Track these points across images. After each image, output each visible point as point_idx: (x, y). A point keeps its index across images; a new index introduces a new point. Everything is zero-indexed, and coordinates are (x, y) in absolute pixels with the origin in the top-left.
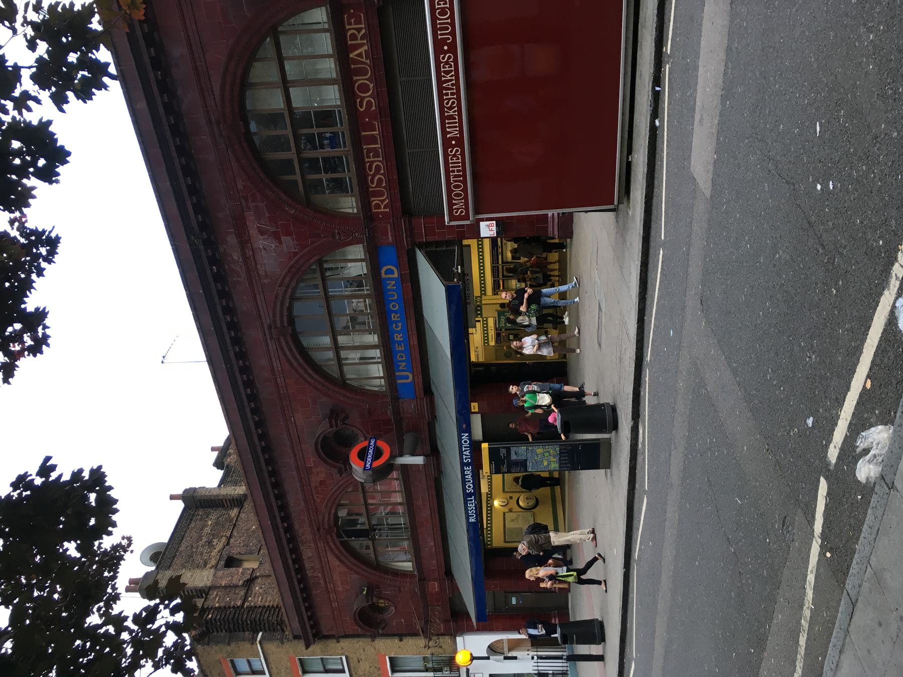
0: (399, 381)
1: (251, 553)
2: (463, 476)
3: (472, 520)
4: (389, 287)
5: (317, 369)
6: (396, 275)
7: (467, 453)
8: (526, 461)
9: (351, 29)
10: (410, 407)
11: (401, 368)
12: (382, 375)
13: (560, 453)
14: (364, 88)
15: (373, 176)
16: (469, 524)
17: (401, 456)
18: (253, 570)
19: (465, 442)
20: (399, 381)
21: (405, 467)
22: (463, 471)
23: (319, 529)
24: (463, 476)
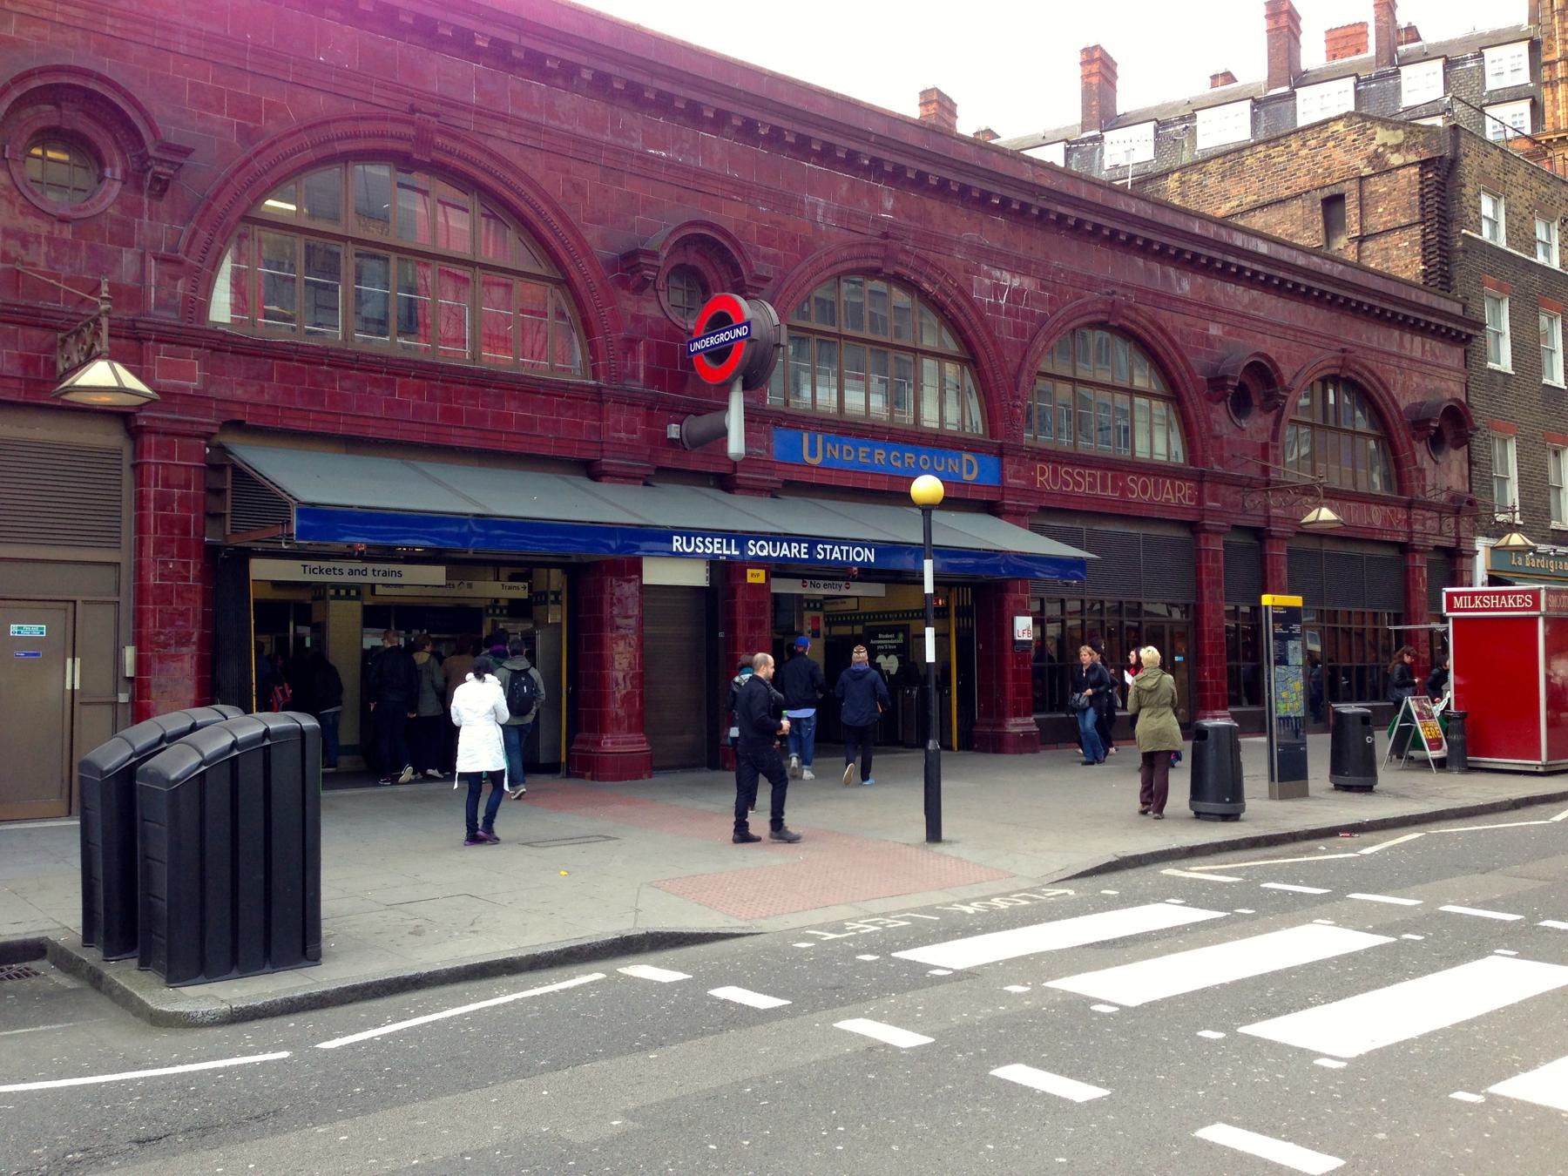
0: (806, 437)
2: (790, 538)
6: (966, 477)
8: (1286, 663)
9: (1187, 488)
11: (829, 447)
14: (1145, 491)
15: (1071, 475)
19: (858, 554)
20: (806, 437)
22: (799, 539)
24: (790, 538)
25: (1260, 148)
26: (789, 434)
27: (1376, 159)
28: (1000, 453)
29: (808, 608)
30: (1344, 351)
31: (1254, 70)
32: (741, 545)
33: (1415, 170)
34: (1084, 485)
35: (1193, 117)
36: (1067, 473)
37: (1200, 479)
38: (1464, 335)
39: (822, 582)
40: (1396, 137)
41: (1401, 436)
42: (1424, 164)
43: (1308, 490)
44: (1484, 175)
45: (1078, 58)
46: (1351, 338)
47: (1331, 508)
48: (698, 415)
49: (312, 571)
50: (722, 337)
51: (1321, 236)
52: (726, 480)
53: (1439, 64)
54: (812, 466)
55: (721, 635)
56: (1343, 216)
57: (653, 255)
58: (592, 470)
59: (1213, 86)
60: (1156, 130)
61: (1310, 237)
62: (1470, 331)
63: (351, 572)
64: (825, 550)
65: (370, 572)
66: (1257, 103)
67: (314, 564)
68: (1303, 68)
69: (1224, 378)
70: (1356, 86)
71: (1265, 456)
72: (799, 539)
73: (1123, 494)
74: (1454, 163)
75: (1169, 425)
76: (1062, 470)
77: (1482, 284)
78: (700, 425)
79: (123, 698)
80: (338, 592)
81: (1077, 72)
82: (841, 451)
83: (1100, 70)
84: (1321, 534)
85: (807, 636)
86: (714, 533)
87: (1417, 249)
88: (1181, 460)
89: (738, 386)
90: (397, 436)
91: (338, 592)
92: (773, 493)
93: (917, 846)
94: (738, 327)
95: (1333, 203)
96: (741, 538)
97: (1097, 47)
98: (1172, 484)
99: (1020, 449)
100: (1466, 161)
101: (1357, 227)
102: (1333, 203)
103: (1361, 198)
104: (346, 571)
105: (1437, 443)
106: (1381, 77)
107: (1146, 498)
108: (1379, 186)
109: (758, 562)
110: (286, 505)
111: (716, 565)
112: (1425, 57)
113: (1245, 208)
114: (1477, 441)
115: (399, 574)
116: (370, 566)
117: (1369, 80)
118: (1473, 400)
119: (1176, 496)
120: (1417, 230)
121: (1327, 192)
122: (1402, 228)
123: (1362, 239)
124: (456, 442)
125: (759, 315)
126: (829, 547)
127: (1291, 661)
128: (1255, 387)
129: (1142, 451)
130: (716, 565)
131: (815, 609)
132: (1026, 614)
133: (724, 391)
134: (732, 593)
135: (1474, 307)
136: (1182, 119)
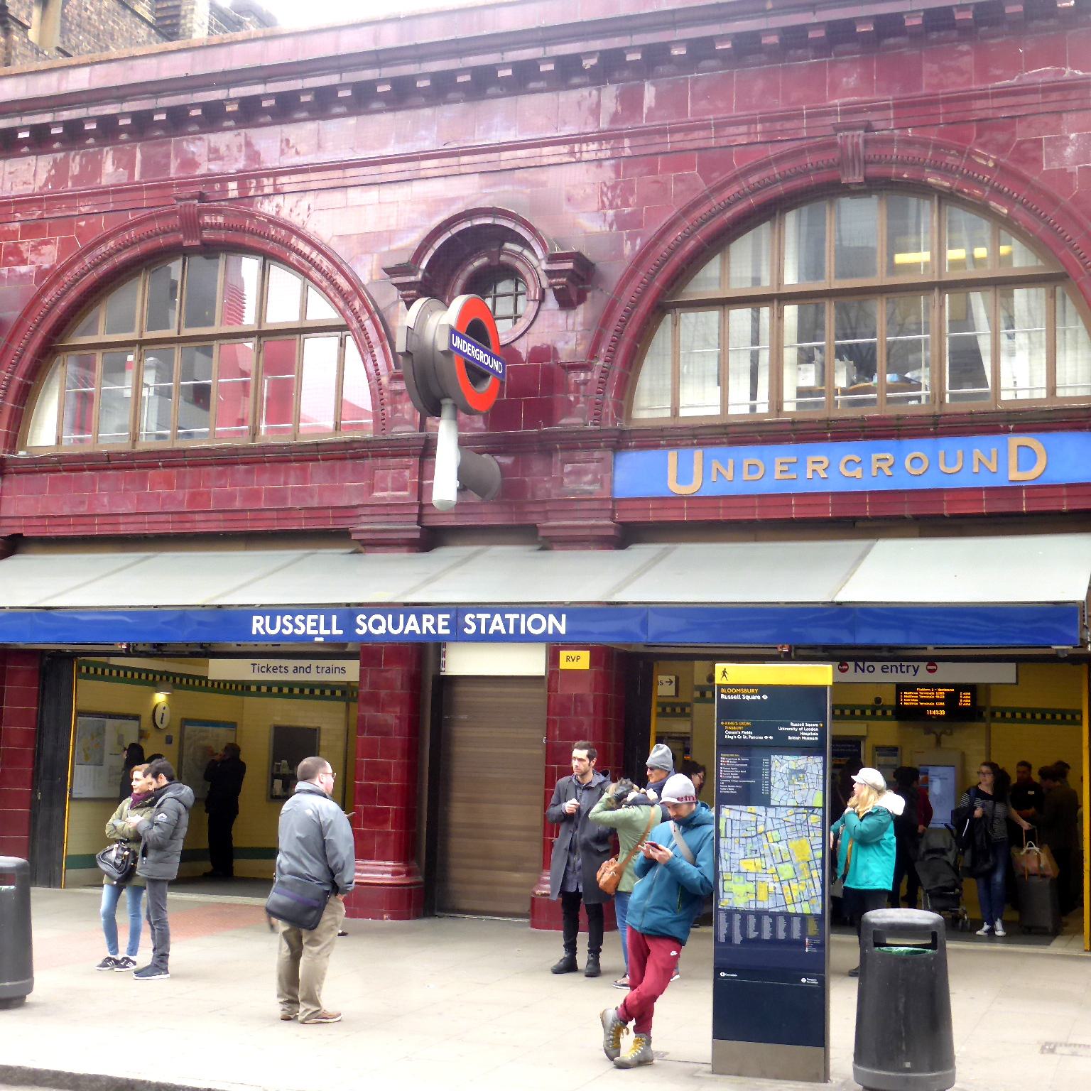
1: (64, 31)
3: (258, 625)
4: (977, 453)
5: (718, 242)
8: (765, 802)
10: (578, 479)
11: (715, 464)
12: (683, 413)
13: (788, 917)
16: (246, 612)
17: (462, 443)
18: (26, 28)
19: (537, 624)
21: (426, 450)
22: (435, 608)
23: (202, 197)
24: (419, 609)
39: (878, 665)
49: (260, 670)
54: (681, 498)
63: (296, 670)
65: (314, 669)
82: (737, 468)
93: (693, 1075)
104: (291, 669)
115: (343, 670)
126: (483, 617)
127: (776, 798)
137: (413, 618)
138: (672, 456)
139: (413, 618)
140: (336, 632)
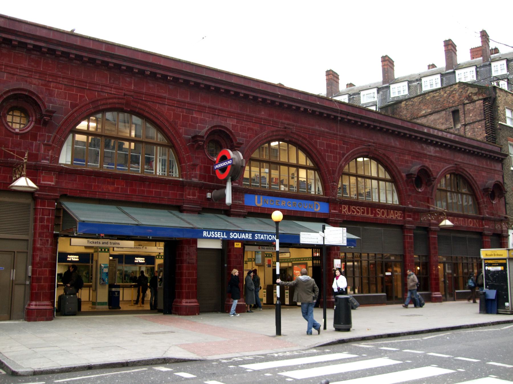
2: (245, 232)
6: (315, 210)
7: (262, 237)
9: (399, 213)
15: (355, 209)
19: (270, 237)
25: (431, 94)
26: (251, 196)
27: (469, 98)
28: (328, 201)
29: (267, 257)
30: (456, 164)
31: (441, 64)
32: (228, 234)
33: (482, 101)
34: (359, 213)
35: (420, 80)
36: (354, 208)
37: (404, 211)
38: (501, 158)
39: (266, 247)
40: (475, 90)
41: (479, 194)
42: (485, 100)
43: (441, 213)
44: (506, 103)
45: (380, 60)
46: (459, 160)
47: (449, 220)
48: (217, 190)
49: (90, 243)
50: (224, 164)
51: (453, 124)
52: (227, 212)
53: (504, 62)
54: (259, 207)
55: (226, 265)
56: (459, 117)
57: (203, 137)
58: (181, 209)
59: (429, 68)
60: (408, 84)
61: (450, 123)
62: (503, 157)
63: (103, 243)
64: (258, 236)
65: (109, 243)
66: (442, 75)
67: (91, 240)
68: (458, 63)
69: (411, 174)
70: (476, 69)
71: (428, 202)
72: (249, 232)
73: (375, 216)
74: (495, 99)
75: (393, 191)
76: (352, 207)
77: (508, 141)
78: (216, 193)
79: (28, 283)
80: (101, 250)
81: (380, 64)
83: (387, 63)
84: (446, 229)
85: (266, 266)
86: (218, 230)
87: (484, 128)
88: (398, 203)
89: (230, 180)
90: (115, 198)
91: (101, 250)
92: (245, 216)
94: (229, 160)
95: (455, 113)
96: (228, 232)
97: (386, 56)
98: (394, 213)
99: (335, 200)
100: (499, 98)
101: (463, 121)
102: (455, 113)
103: (464, 111)
104: (101, 243)
105: (492, 196)
106: (484, 66)
107: (384, 217)
108: (470, 107)
109: (238, 240)
110: (76, 221)
111: (224, 241)
112: (500, 59)
113: (427, 114)
114: (507, 195)
116: (109, 241)
117: (480, 67)
118: (506, 181)
119: (396, 216)
120: (483, 122)
121: (453, 109)
122: (479, 121)
123: (465, 125)
124: (135, 200)
125: (236, 156)
126: (259, 235)
128: (423, 178)
129: (383, 200)
130: (224, 241)
131: (269, 257)
132: (339, 258)
133: (225, 181)
134: (230, 251)
135: (504, 148)
136: (417, 80)
137: (243, 234)
138: (256, 197)
139: (243, 234)
140: (226, 237)
